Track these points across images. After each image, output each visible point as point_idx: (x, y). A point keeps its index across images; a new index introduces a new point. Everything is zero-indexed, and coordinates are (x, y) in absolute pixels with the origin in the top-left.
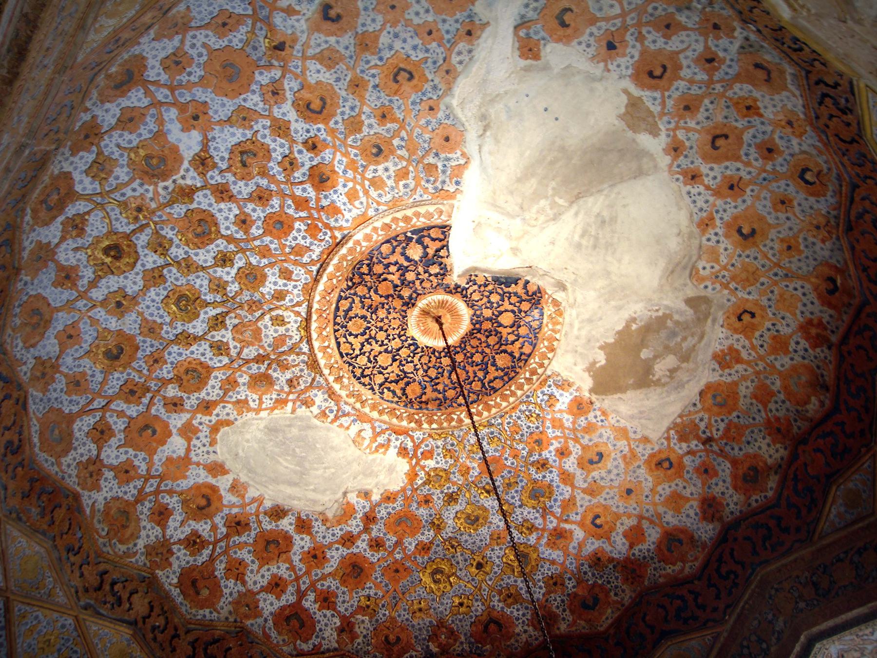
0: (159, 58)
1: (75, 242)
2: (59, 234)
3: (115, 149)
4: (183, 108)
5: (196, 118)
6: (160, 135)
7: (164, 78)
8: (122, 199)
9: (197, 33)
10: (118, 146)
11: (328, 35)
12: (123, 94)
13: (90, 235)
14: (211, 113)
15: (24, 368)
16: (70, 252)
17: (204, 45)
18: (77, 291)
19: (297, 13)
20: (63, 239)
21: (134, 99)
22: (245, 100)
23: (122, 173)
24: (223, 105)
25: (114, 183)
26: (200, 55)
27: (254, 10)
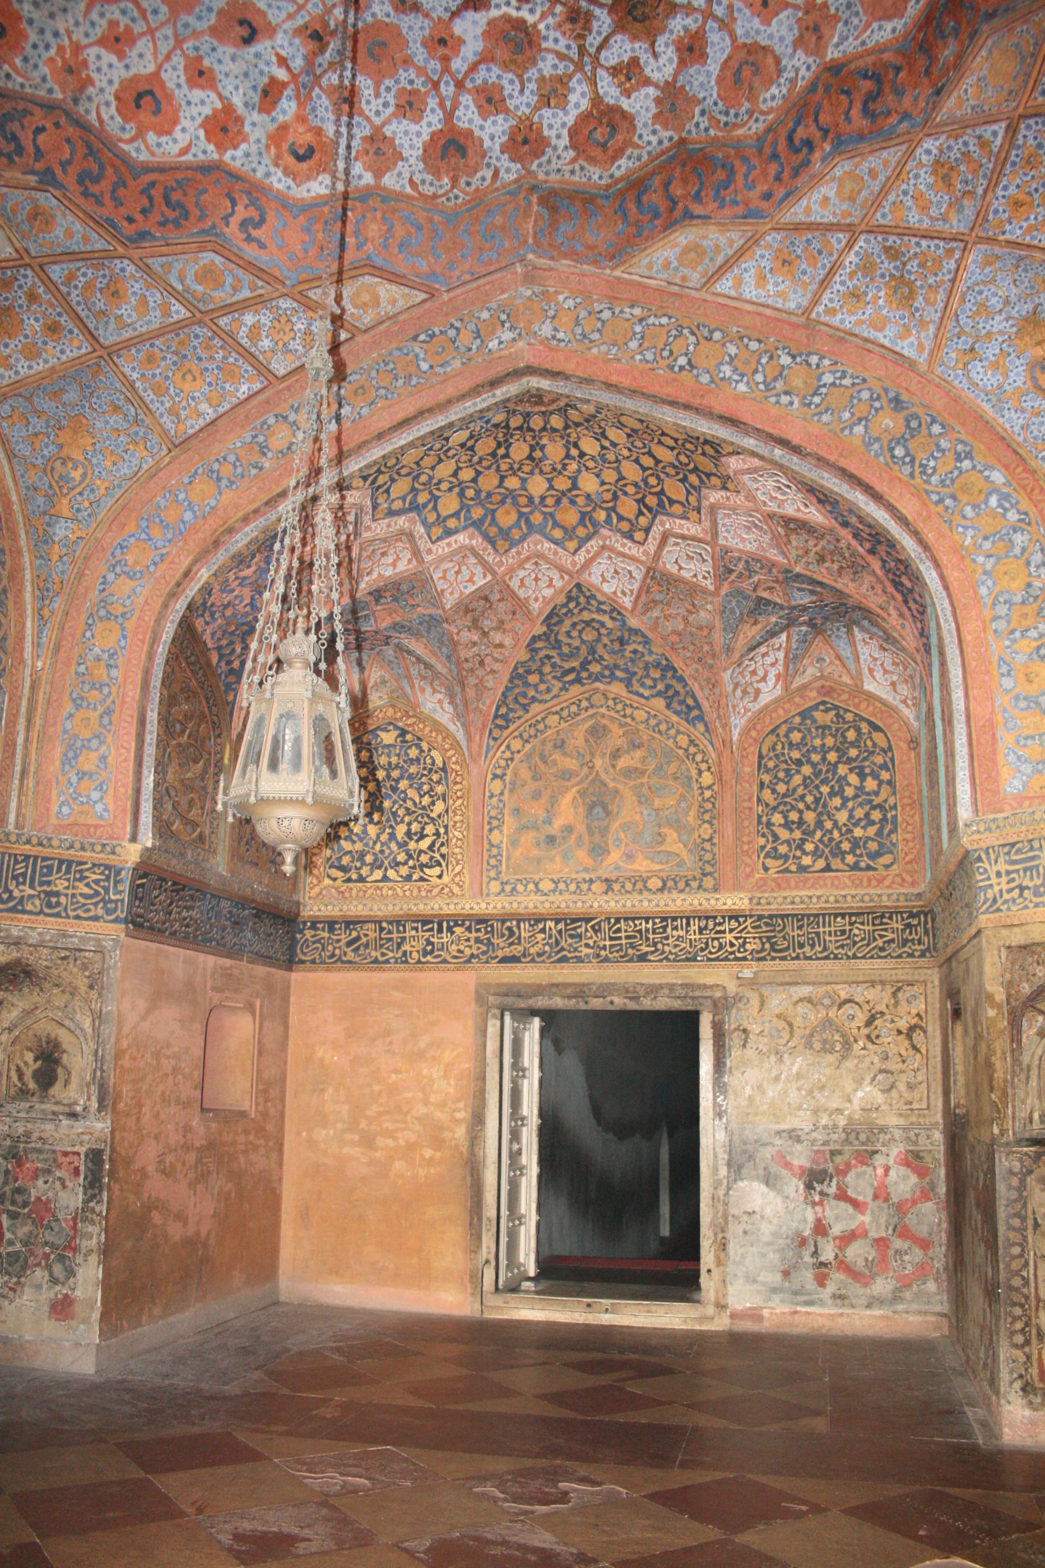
0: (417, 128)
1: (647, 63)
2: (644, 91)
3: (527, 92)
4: (446, 60)
5: (442, 42)
6: (485, 58)
7: (432, 102)
8: (574, 46)
9: (372, 115)
10: (522, 91)
11: (264, 14)
12: (469, 133)
13: (633, 50)
14: (427, 32)
15: (803, 72)
16: (661, 61)
17: (377, 95)
18: (705, 23)
19: (277, 55)
20: (647, 82)
21: (469, 114)
22: (388, 15)
23: (547, 65)
24: (410, 28)
25: (561, 66)
26: (388, 89)
27: (312, 89)
